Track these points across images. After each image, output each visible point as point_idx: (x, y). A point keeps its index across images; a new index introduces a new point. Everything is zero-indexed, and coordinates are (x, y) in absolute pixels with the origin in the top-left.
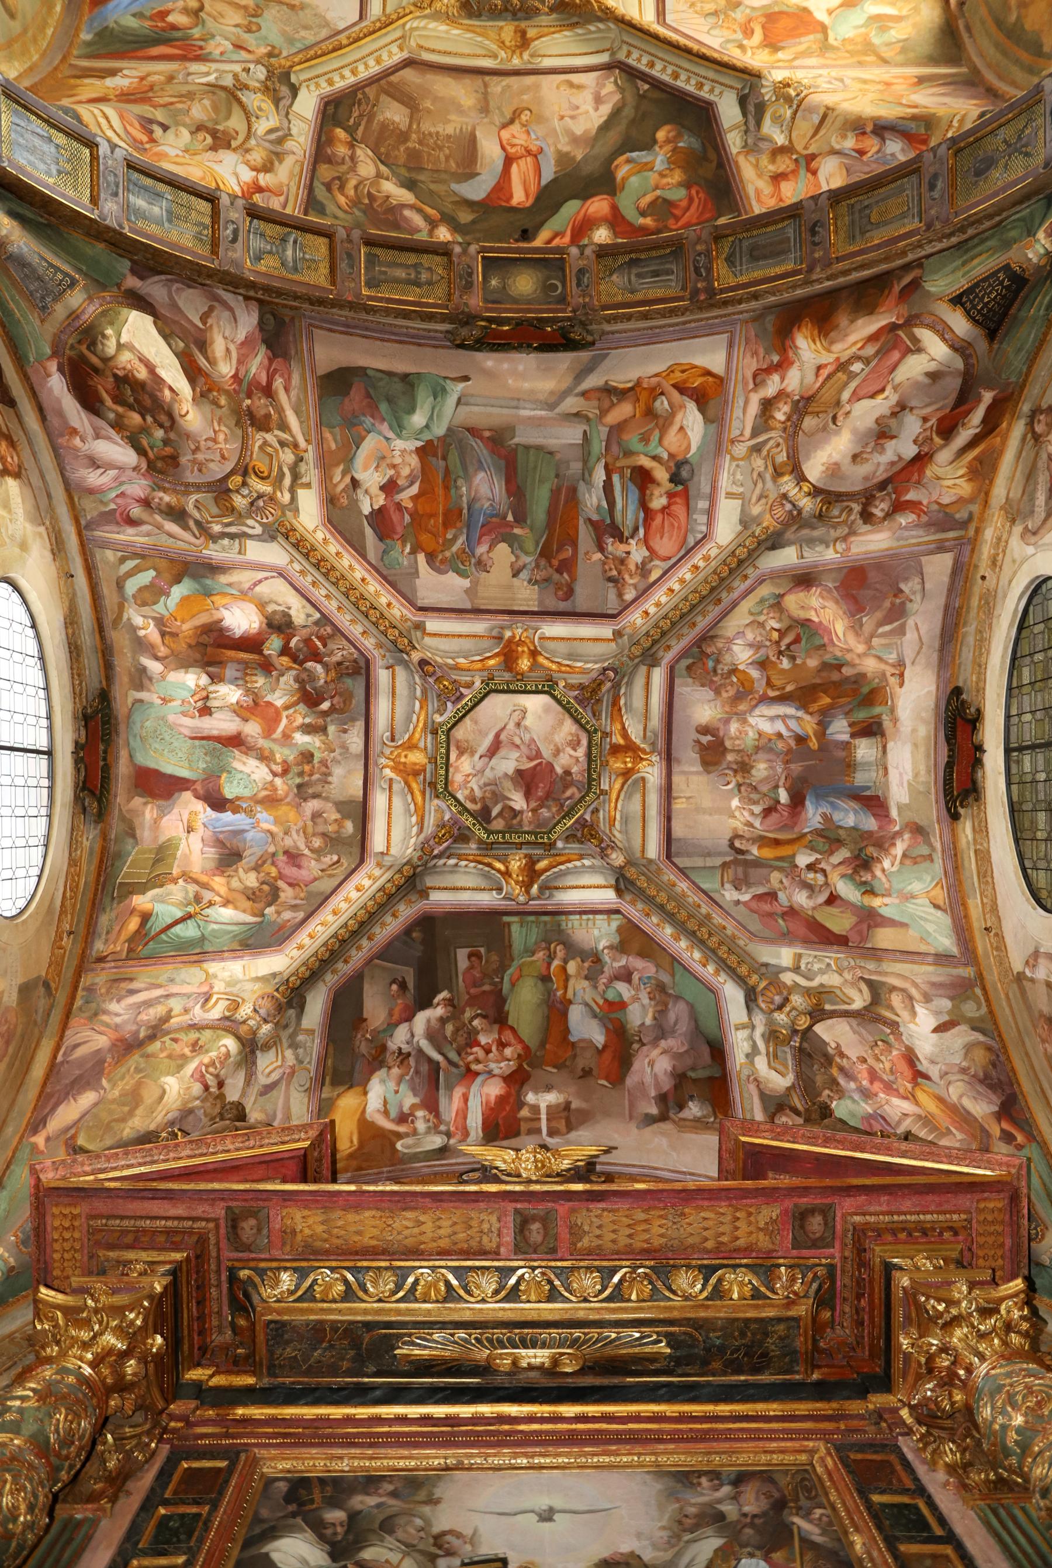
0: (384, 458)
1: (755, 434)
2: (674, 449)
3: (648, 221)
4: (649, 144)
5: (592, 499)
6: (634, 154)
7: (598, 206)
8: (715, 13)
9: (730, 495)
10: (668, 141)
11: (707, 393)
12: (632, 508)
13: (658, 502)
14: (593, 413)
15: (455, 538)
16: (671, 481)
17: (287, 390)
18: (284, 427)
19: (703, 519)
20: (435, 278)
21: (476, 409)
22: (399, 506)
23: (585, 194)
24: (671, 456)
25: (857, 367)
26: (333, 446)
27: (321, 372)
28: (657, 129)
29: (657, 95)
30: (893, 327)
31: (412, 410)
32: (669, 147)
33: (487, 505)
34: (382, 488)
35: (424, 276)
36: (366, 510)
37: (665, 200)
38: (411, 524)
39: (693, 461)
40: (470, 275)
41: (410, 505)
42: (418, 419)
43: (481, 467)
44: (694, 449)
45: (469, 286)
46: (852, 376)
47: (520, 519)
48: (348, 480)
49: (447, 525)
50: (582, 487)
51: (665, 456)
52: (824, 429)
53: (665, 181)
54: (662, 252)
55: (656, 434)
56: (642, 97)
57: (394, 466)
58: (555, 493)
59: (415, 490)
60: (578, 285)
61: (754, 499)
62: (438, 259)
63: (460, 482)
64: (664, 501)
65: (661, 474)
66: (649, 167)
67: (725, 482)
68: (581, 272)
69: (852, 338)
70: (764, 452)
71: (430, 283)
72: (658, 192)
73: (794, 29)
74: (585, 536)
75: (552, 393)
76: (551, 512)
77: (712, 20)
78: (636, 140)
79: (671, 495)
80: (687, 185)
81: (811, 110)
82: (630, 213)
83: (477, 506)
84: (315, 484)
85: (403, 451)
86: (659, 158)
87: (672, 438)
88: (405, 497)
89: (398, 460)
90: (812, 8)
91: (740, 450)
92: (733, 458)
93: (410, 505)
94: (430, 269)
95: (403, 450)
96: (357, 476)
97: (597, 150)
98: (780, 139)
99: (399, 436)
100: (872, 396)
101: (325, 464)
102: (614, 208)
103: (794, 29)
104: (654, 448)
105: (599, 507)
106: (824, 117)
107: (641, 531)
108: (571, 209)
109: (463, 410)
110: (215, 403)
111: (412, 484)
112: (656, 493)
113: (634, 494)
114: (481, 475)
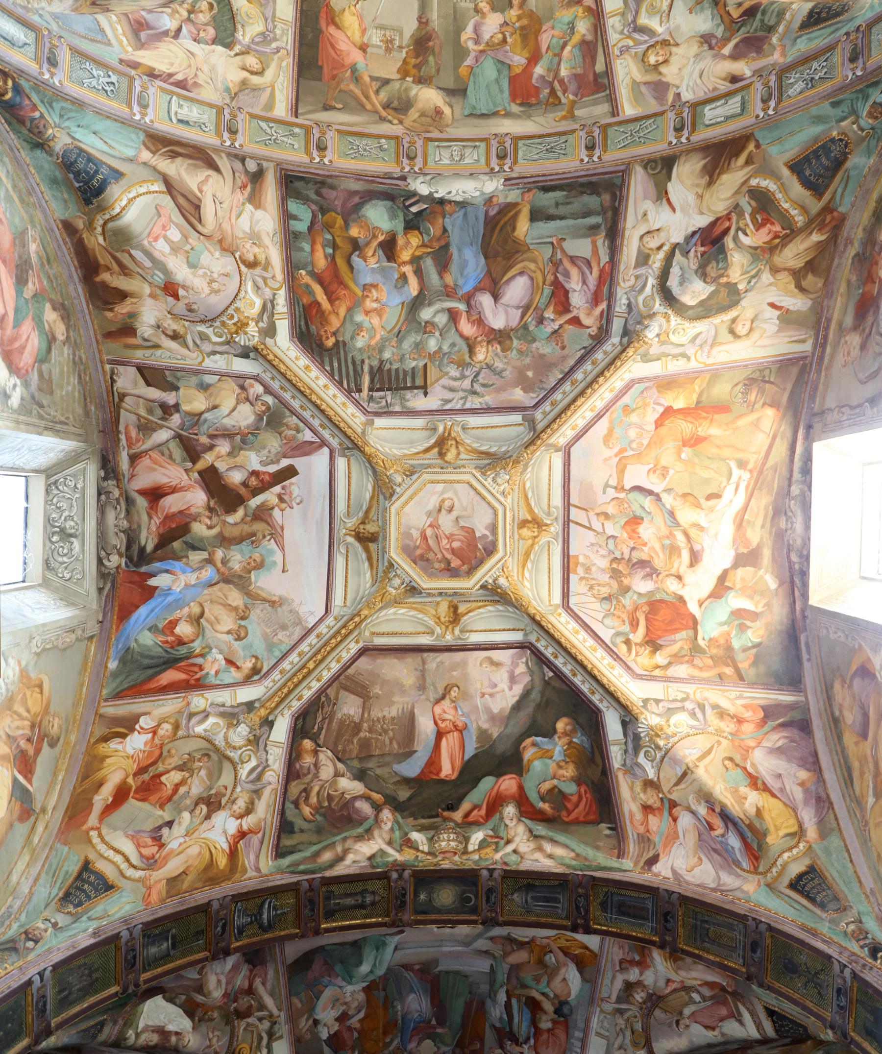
0: (337, 1000)
1: (619, 1000)
2: (558, 992)
3: (546, 807)
4: (550, 733)
5: (496, 1012)
6: (539, 739)
7: (508, 784)
8: (608, 598)
9: (598, 1034)
10: (565, 734)
11: (585, 963)
12: (525, 1024)
13: (545, 1024)
14: (498, 953)
15: (392, 1041)
16: (555, 1012)
17: (264, 984)
18: (262, 1007)
19: (579, 1044)
20: (377, 898)
21: (408, 951)
22: (349, 1029)
23: (498, 772)
24: (556, 996)
25: (696, 997)
26: (299, 1005)
27: (289, 961)
28: (557, 720)
29: (557, 684)
30: (723, 989)
31: (361, 963)
32: (565, 740)
33: (416, 1015)
34: (337, 1020)
35: (369, 899)
36: (324, 1035)
37: (560, 791)
38: (358, 1038)
39: (573, 1003)
40: (404, 895)
41: (358, 1026)
42: (365, 968)
43: (412, 990)
44: (573, 996)
45: (403, 904)
46: (692, 1001)
47: (441, 1023)
48: (311, 1022)
49: (385, 1033)
50: (489, 1002)
51: (552, 995)
52: (670, 1025)
53: (561, 772)
54: (552, 883)
55: (545, 979)
56: (547, 683)
57: (346, 1003)
58: (468, 1006)
59: (362, 1015)
60: (488, 901)
61: (616, 1046)
62: (379, 882)
63: (395, 1003)
64: (549, 1025)
65: (548, 1006)
66: (547, 755)
67: (595, 1023)
68: (490, 891)
69: (694, 974)
70: (626, 1017)
71: (373, 904)
72: (555, 782)
73: (672, 622)
74: (490, 1037)
75: (467, 936)
76: (465, 1017)
77: (606, 605)
78: (540, 728)
79: (554, 1022)
80: (578, 781)
81: (676, 761)
82: (533, 796)
83: (409, 1017)
84: (285, 1036)
85: (353, 993)
86: (558, 747)
87: (557, 983)
88: (354, 1022)
89: (348, 999)
90: (687, 598)
91: (609, 1007)
92: (602, 1011)
93: (358, 1026)
94: (373, 893)
95: (352, 992)
96: (317, 1017)
97: (509, 730)
98: (651, 774)
99: (350, 983)
100: (707, 1027)
101: (293, 1020)
102: (521, 788)
103: (672, 622)
104: (543, 987)
105: (501, 1019)
106: (684, 775)
107: (532, 1041)
108: (487, 784)
109: (399, 954)
110: (211, 1020)
111: (359, 1011)
112: (544, 1018)
113: (527, 1015)
114: (412, 996)
